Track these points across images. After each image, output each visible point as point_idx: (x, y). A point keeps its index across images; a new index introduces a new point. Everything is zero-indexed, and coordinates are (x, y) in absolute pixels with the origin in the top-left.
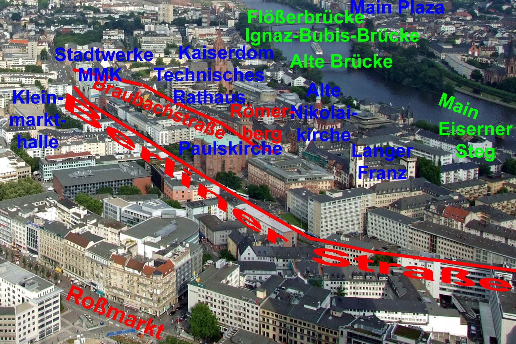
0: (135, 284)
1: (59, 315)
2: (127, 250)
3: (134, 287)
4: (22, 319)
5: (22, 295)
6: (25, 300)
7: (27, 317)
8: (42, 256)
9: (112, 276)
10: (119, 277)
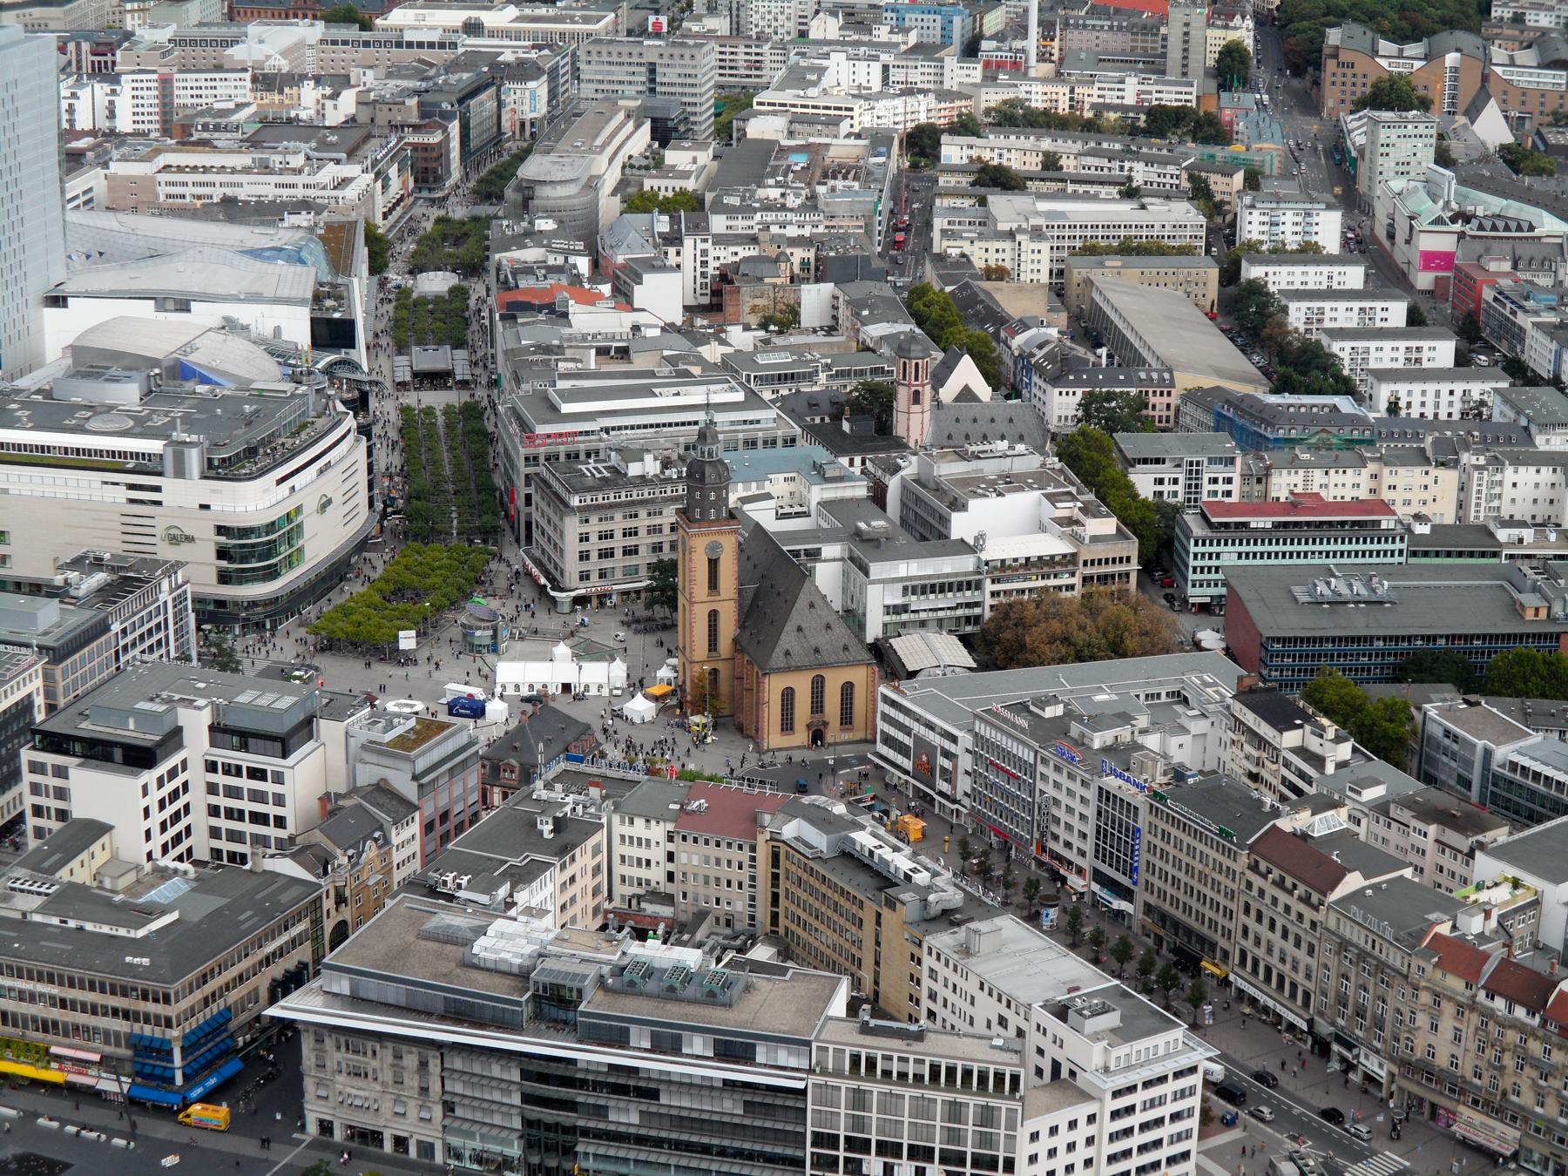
0: (1508, 1060)
1: (1191, 1144)
2: (1493, 923)
3: (1502, 1068)
4: (1045, 1143)
5: (1052, 1052)
6: (1064, 1074)
7: (1064, 1137)
8: (1149, 909)
9: (1422, 1020)
10: (1447, 1023)
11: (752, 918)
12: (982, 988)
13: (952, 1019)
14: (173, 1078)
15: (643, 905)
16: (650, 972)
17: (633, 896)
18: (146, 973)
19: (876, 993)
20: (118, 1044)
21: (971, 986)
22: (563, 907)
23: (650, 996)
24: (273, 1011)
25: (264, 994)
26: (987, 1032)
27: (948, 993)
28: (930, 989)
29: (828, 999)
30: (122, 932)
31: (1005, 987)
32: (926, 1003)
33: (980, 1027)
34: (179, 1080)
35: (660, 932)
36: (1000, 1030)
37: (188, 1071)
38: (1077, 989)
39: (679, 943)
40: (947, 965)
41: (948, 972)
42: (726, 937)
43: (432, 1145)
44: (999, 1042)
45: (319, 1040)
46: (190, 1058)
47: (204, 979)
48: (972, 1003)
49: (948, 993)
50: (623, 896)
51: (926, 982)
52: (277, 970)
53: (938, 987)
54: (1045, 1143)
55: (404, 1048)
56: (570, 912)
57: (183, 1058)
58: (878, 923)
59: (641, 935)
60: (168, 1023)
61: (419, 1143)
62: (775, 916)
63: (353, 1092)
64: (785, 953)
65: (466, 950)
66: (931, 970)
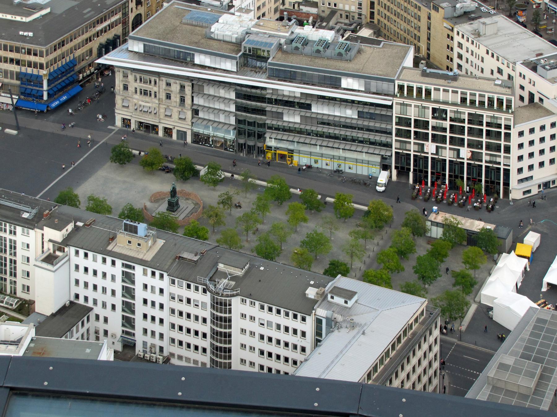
4: (527, 137)
5: (529, 88)
6: (536, 100)
11: (360, 15)
12: (488, 53)
13: (471, 69)
14: (42, 96)
15: (301, 7)
16: (306, 42)
17: (296, 3)
18: (31, 40)
19: (429, 55)
20: (12, 78)
21: (482, 52)
22: (259, 8)
23: (306, 55)
24: (100, 61)
25: (95, 51)
26: (491, 76)
27: (468, 55)
28: (459, 54)
29: (403, 57)
30: (18, 18)
31: (500, 52)
32: (456, 60)
33: (487, 74)
34: (45, 97)
35: (310, 21)
36: (499, 76)
37: (51, 92)
38: (541, 54)
39: (321, 27)
40: (468, 41)
41: (469, 45)
42: (346, 24)
43: (185, 133)
44: (499, 82)
45: (125, 76)
46: (53, 85)
47: (62, 44)
48: (482, 61)
49: (468, 55)
50: (290, 3)
51: (456, 50)
52: (103, 39)
53: (463, 52)
54: (527, 137)
55: (172, 81)
56: (262, 11)
57: (48, 86)
58: (429, 18)
59: (301, 24)
60: (42, 67)
61: (178, 131)
62: (372, 14)
63: (143, 104)
64: (378, 33)
65: (207, 30)
66: (459, 43)
